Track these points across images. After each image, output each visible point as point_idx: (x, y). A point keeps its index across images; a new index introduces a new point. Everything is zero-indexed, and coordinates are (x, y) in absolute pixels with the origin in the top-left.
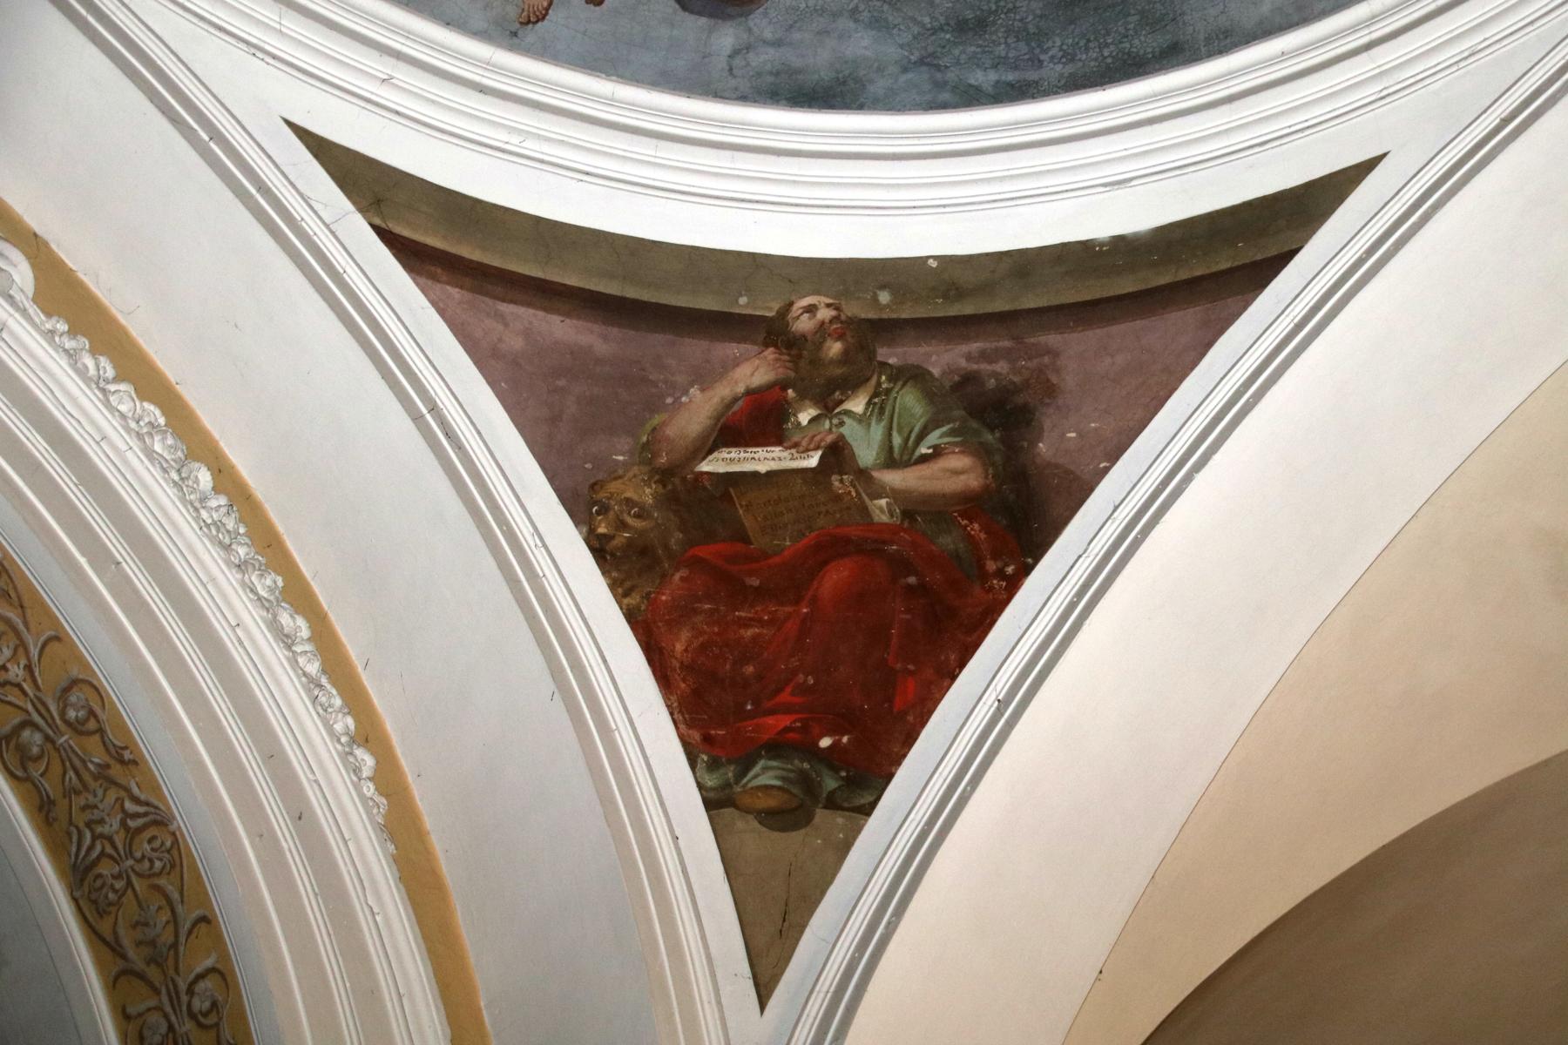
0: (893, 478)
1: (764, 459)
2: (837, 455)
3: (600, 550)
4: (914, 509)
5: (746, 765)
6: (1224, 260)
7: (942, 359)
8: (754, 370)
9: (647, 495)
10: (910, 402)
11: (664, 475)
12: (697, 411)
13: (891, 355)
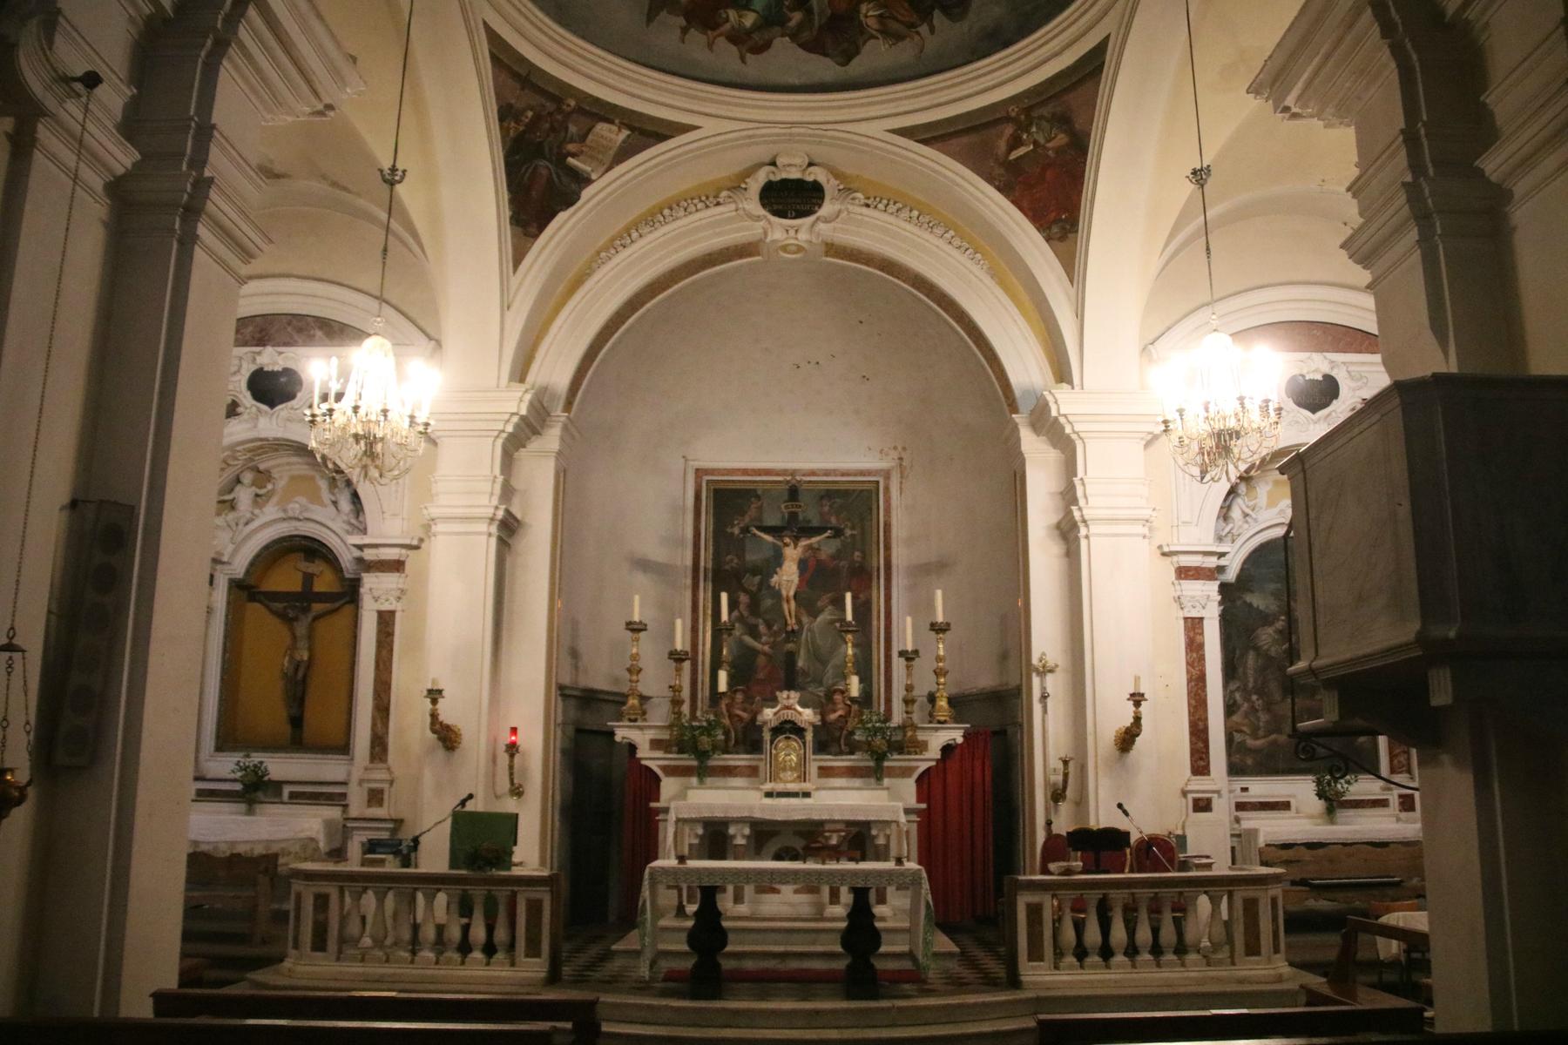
0: (1050, 145)
1: (1021, 151)
2: (1035, 143)
3: (999, 189)
4: (1058, 151)
5: (1049, 228)
6: (1090, 71)
7: (1046, 111)
8: (1009, 130)
9: (1002, 171)
10: (1044, 124)
11: (1001, 165)
12: (1002, 145)
13: (1035, 114)
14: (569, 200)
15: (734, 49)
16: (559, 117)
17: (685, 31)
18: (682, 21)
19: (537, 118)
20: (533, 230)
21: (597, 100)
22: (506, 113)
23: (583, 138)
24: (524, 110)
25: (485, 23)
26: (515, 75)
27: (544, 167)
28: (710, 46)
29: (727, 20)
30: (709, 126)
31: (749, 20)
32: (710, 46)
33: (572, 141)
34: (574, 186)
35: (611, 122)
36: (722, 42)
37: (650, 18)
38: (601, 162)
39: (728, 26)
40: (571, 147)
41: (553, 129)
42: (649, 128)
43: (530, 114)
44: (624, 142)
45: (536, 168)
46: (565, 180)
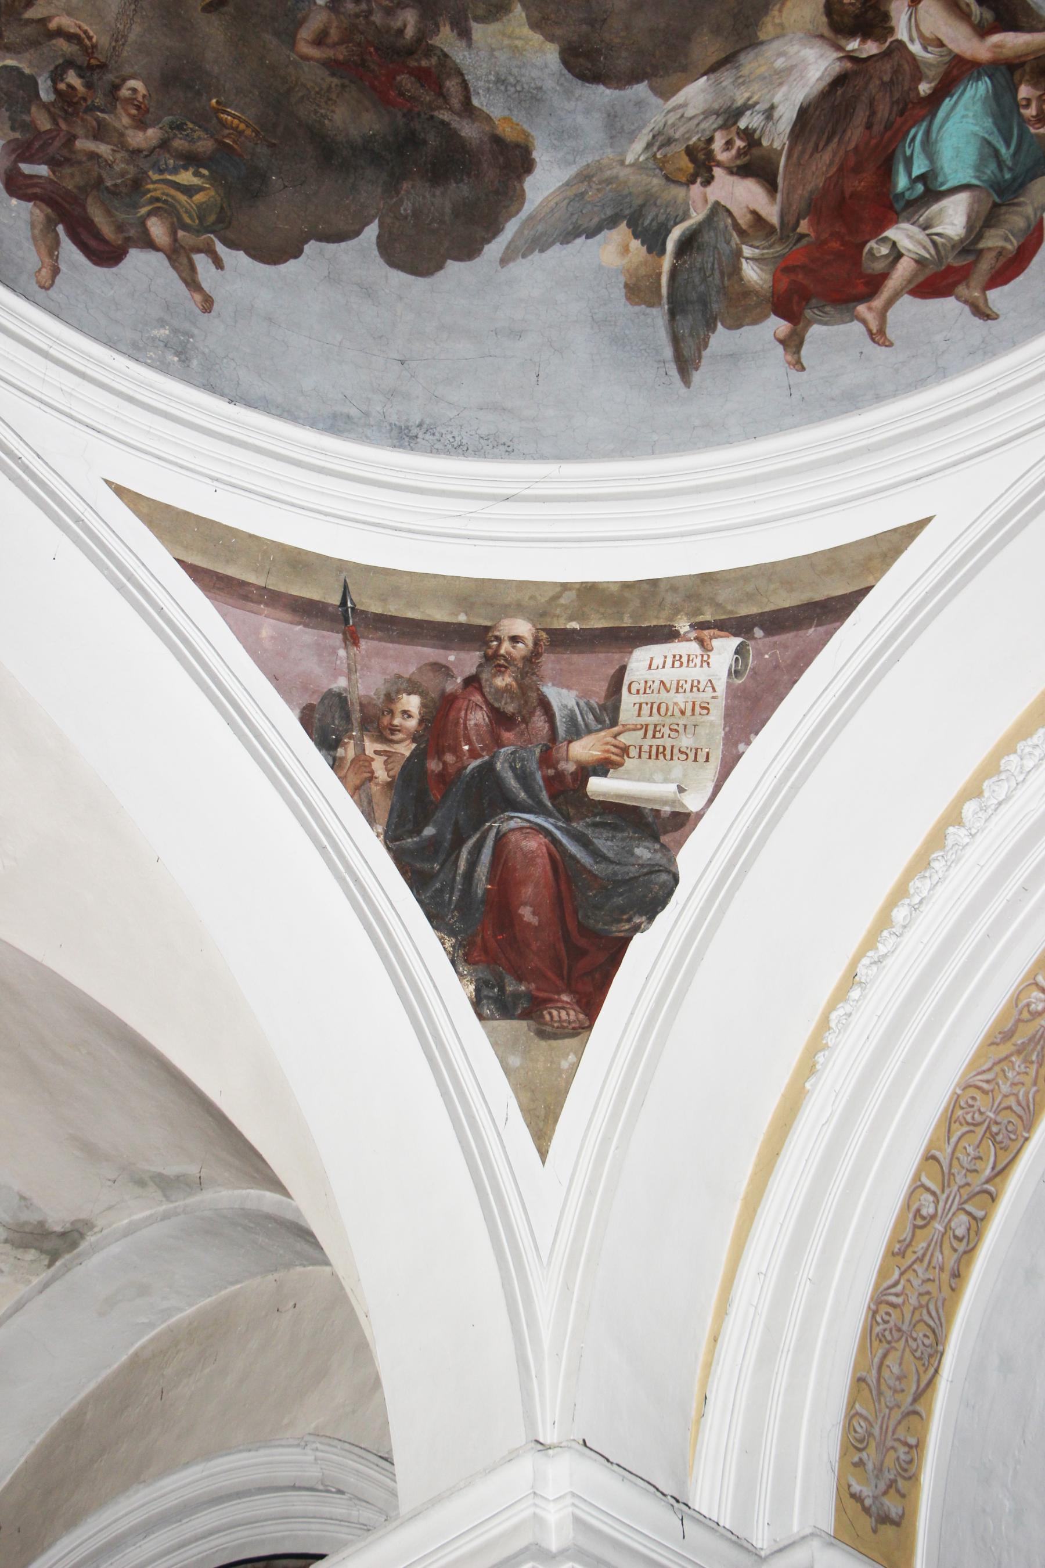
14: (651, 893)
15: (949, 305)
16: (500, 682)
17: (793, 343)
18: (776, 325)
19: (440, 715)
20: (566, 1013)
21: (589, 591)
22: (328, 723)
23: (608, 712)
24: (390, 698)
25: (120, 491)
26: (307, 611)
27: (528, 833)
28: (879, 336)
29: (897, 255)
30: (956, 506)
31: (953, 217)
32: (879, 336)
33: (576, 732)
34: (643, 852)
35: (669, 635)
36: (909, 313)
37: (685, 364)
38: (695, 755)
39: (904, 268)
40: (584, 749)
41: (501, 719)
42: (785, 600)
43: (412, 703)
44: (735, 673)
45: (501, 839)
46: (604, 843)
